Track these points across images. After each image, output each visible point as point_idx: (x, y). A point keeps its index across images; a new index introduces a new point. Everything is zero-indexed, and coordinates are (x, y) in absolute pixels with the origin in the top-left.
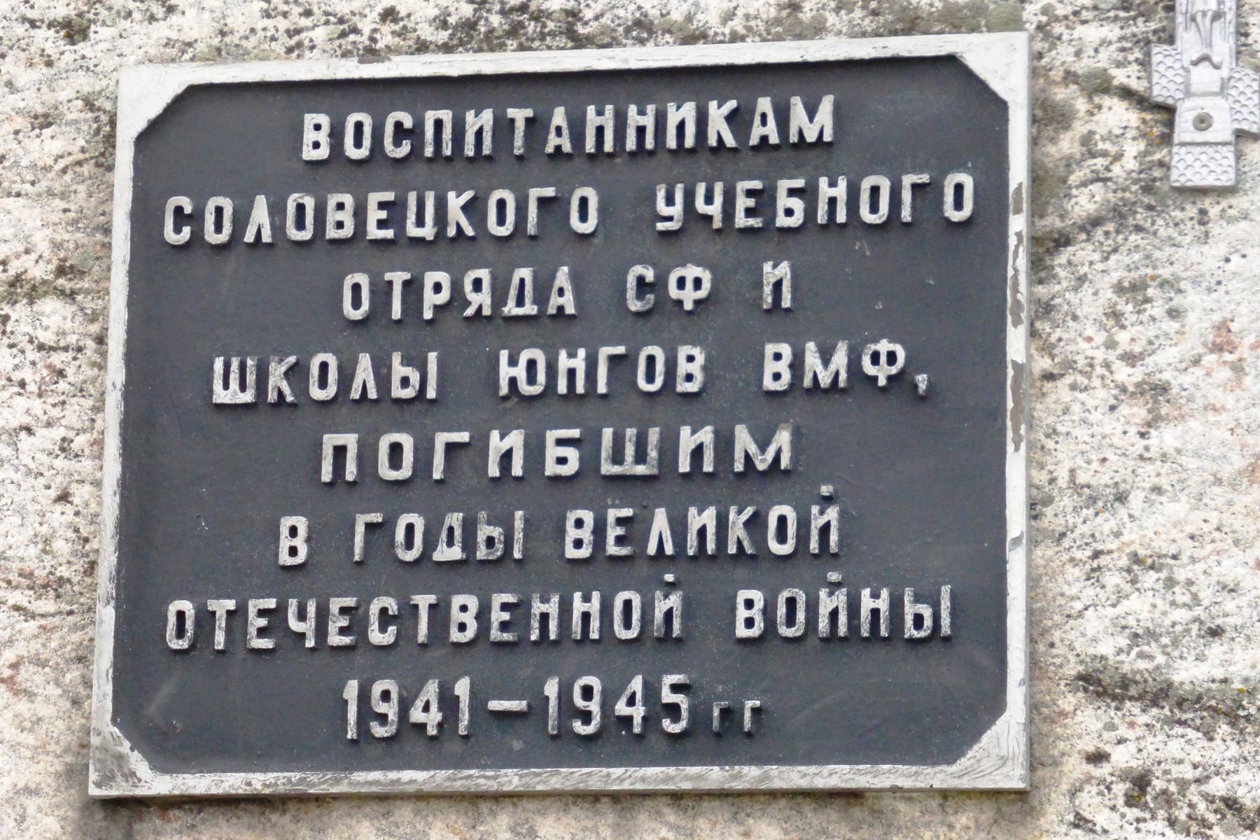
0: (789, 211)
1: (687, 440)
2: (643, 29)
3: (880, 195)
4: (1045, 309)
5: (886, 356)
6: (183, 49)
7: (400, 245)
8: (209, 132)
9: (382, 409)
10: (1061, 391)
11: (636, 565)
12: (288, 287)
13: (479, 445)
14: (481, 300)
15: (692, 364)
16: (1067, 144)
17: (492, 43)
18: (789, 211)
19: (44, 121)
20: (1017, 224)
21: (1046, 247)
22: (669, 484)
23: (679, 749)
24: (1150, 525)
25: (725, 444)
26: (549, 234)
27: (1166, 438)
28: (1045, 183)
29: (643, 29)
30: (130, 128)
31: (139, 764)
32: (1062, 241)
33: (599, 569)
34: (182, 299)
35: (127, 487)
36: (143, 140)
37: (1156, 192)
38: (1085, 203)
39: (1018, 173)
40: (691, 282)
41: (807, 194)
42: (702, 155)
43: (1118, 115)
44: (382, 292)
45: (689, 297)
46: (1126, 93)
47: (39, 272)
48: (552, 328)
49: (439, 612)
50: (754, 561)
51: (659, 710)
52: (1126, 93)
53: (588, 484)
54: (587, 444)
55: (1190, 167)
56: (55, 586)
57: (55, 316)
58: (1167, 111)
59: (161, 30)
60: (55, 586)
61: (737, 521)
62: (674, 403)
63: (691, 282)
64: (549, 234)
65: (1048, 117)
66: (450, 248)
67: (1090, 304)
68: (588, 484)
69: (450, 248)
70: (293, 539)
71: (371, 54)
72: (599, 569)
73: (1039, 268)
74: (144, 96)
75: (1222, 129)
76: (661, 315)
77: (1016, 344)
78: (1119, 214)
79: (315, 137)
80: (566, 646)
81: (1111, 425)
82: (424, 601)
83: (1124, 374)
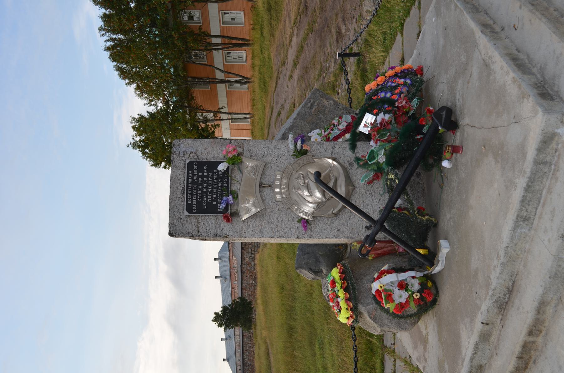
0: (196, 173)
3: (196, 168)
5: (205, 168)
7: (197, 197)
9: (207, 198)
11: (217, 182)
12: (199, 204)
15: (205, 179)
18: (196, 173)
22: (213, 180)
23: (228, 180)
26: (197, 188)
30: (188, 214)
33: (217, 184)
34: (200, 210)
35: (211, 213)
37: (196, 153)
38: (196, 157)
40: (200, 179)
42: (193, 179)
48: (202, 188)
53: (212, 185)
62: (208, 180)
63: (200, 179)
64: (197, 188)
67: (202, 157)
68: (212, 185)
70: (215, 203)
72: (217, 184)
74: (186, 213)
76: (202, 181)
79: (190, 202)
80: (222, 186)
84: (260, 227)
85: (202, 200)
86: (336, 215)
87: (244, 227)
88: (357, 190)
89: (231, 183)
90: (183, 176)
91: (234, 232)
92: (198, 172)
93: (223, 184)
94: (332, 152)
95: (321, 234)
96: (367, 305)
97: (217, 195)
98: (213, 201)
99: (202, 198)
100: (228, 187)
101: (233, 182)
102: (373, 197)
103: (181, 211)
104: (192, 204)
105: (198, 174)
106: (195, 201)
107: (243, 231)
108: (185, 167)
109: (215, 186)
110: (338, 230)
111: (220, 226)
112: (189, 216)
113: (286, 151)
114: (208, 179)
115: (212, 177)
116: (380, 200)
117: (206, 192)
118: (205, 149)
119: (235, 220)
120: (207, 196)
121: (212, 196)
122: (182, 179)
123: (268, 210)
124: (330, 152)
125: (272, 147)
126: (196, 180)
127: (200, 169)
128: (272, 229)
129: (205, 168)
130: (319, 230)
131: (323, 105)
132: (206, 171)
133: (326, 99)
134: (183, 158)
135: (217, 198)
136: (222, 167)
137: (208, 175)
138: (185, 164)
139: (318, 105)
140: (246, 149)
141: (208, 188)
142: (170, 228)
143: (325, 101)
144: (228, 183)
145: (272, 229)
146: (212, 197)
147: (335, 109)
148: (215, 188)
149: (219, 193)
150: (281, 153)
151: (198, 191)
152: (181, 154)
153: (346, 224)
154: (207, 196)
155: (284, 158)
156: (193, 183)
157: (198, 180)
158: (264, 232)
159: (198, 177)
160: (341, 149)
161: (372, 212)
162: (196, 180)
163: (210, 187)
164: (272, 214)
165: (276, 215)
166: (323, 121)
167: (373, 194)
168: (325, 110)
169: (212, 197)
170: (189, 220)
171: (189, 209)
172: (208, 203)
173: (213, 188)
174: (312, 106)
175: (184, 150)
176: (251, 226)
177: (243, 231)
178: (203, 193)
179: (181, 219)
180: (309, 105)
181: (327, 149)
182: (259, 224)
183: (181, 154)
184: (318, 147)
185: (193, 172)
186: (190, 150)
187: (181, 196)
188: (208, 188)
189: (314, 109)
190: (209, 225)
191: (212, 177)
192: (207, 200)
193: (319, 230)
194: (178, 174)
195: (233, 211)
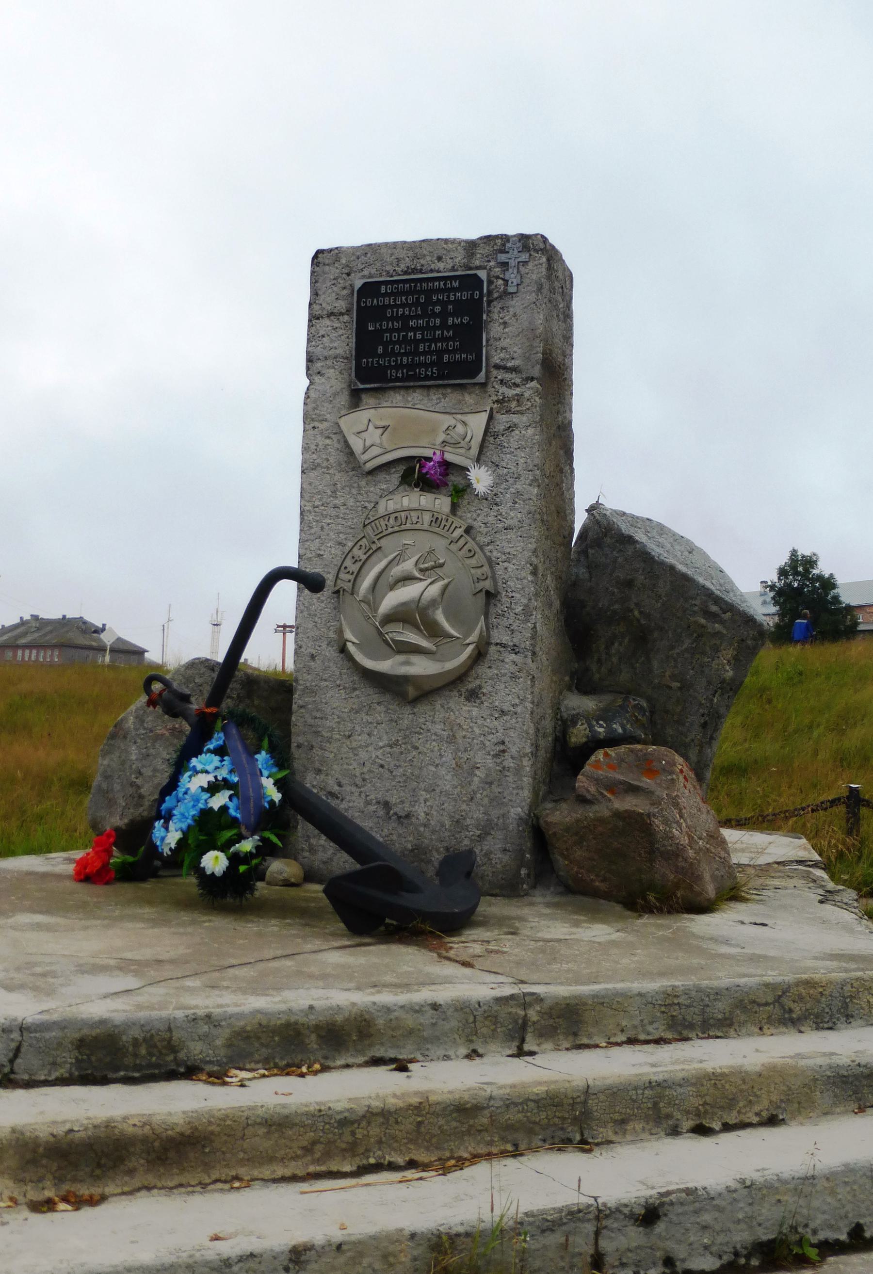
0: (452, 298)
1: (437, 333)
2: (432, 271)
3: (465, 295)
4: (490, 312)
5: (466, 320)
6: (364, 277)
7: (396, 306)
9: (393, 330)
10: (492, 324)
11: (430, 352)
13: (407, 334)
14: (407, 313)
15: (438, 321)
16: (493, 287)
17: (410, 274)
18: (452, 298)
19: (344, 288)
20: (485, 299)
21: (489, 302)
22: (435, 340)
24: (504, 343)
25: (443, 333)
26: (417, 303)
27: (507, 330)
28: (490, 292)
29: (432, 271)
30: (356, 289)
31: (359, 384)
32: (492, 301)
33: (424, 353)
35: (356, 342)
36: (358, 291)
37: (506, 293)
38: (496, 295)
39: (485, 291)
40: (438, 309)
41: (455, 295)
42: (440, 291)
43: (500, 282)
44: (393, 312)
45: (438, 311)
46: (502, 279)
47: (344, 311)
48: (417, 317)
49: (401, 360)
50: (447, 351)
51: (432, 373)
52: (502, 279)
53: (423, 340)
54: (423, 334)
55: (512, 289)
56: (347, 358)
57: (346, 318)
58: (507, 281)
59: (361, 274)
60: (347, 358)
61: (444, 345)
62: (435, 328)
63: (438, 309)
64: (417, 303)
65: (490, 282)
66: (403, 306)
67: (496, 310)
68: (423, 340)
69: (403, 306)
70: (380, 350)
71: (392, 276)
72: (424, 353)
73: (489, 305)
74: (358, 284)
75: (515, 284)
76: (434, 315)
77: (485, 317)
78: (500, 297)
79: (383, 290)
80: (420, 365)
81: (499, 329)
83: (501, 321)
84: (325, 464)
85: (388, 319)
86: (343, 650)
88: (408, 709)
89: (428, 387)
90: (449, 266)
91: (315, 401)
92: (456, 302)
93: (425, 365)
94: (504, 646)
95: (305, 613)
96: (136, 717)
97: (399, 354)
98: (385, 345)
99: (393, 318)
102: (388, 749)
103: (366, 272)
104: (378, 295)
105: (449, 302)
106: (387, 302)
107: (316, 424)
108: (470, 269)
109: (421, 348)
110: (313, 657)
112: (353, 291)
113: (508, 523)
114: (438, 328)
115: (443, 339)
116: (382, 766)
117: (406, 328)
120: (398, 330)
122: (441, 265)
123: (363, 483)
124: (505, 639)
125: (518, 486)
126: (435, 298)
127: (461, 308)
128: (319, 493)
129: (466, 320)
130: (313, 608)
131: (716, 649)
132: (457, 321)
133: (736, 658)
134: (492, 263)
135: (393, 354)
137: (449, 328)
138: (478, 268)
139: (717, 634)
140: (515, 418)
141: (414, 329)
142: (330, 251)
143: (728, 653)
145: (319, 493)
146: (395, 343)
147: (709, 683)
148: (417, 347)
149: (405, 359)
150: (503, 510)
151: (410, 306)
152: (502, 257)
153: (326, 676)
154: (398, 330)
155: (491, 519)
156: (429, 293)
157: (436, 304)
158: (313, 474)
159: (444, 304)
160: (513, 668)
161: (354, 744)
162: (435, 298)
164: (354, 491)
165: (351, 502)
166: (672, 648)
167: (396, 750)
168: (703, 653)
169: (395, 343)
170: (345, 292)
171: (369, 289)
172: (379, 332)
173: (417, 342)
174: (707, 614)
175: (512, 263)
176: (328, 441)
177: (316, 424)
178: (405, 319)
179: (348, 274)
180: (714, 608)
181: (513, 631)
182: (332, 460)
183: (502, 257)
184: (519, 609)
185: (453, 289)
186: (512, 276)
187: (403, 266)
188: (414, 329)
189: (703, 621)
190: (332, 341)
191: (443, 339)
192: (387, 330)
193: (313, 608)
194: (453, 255)
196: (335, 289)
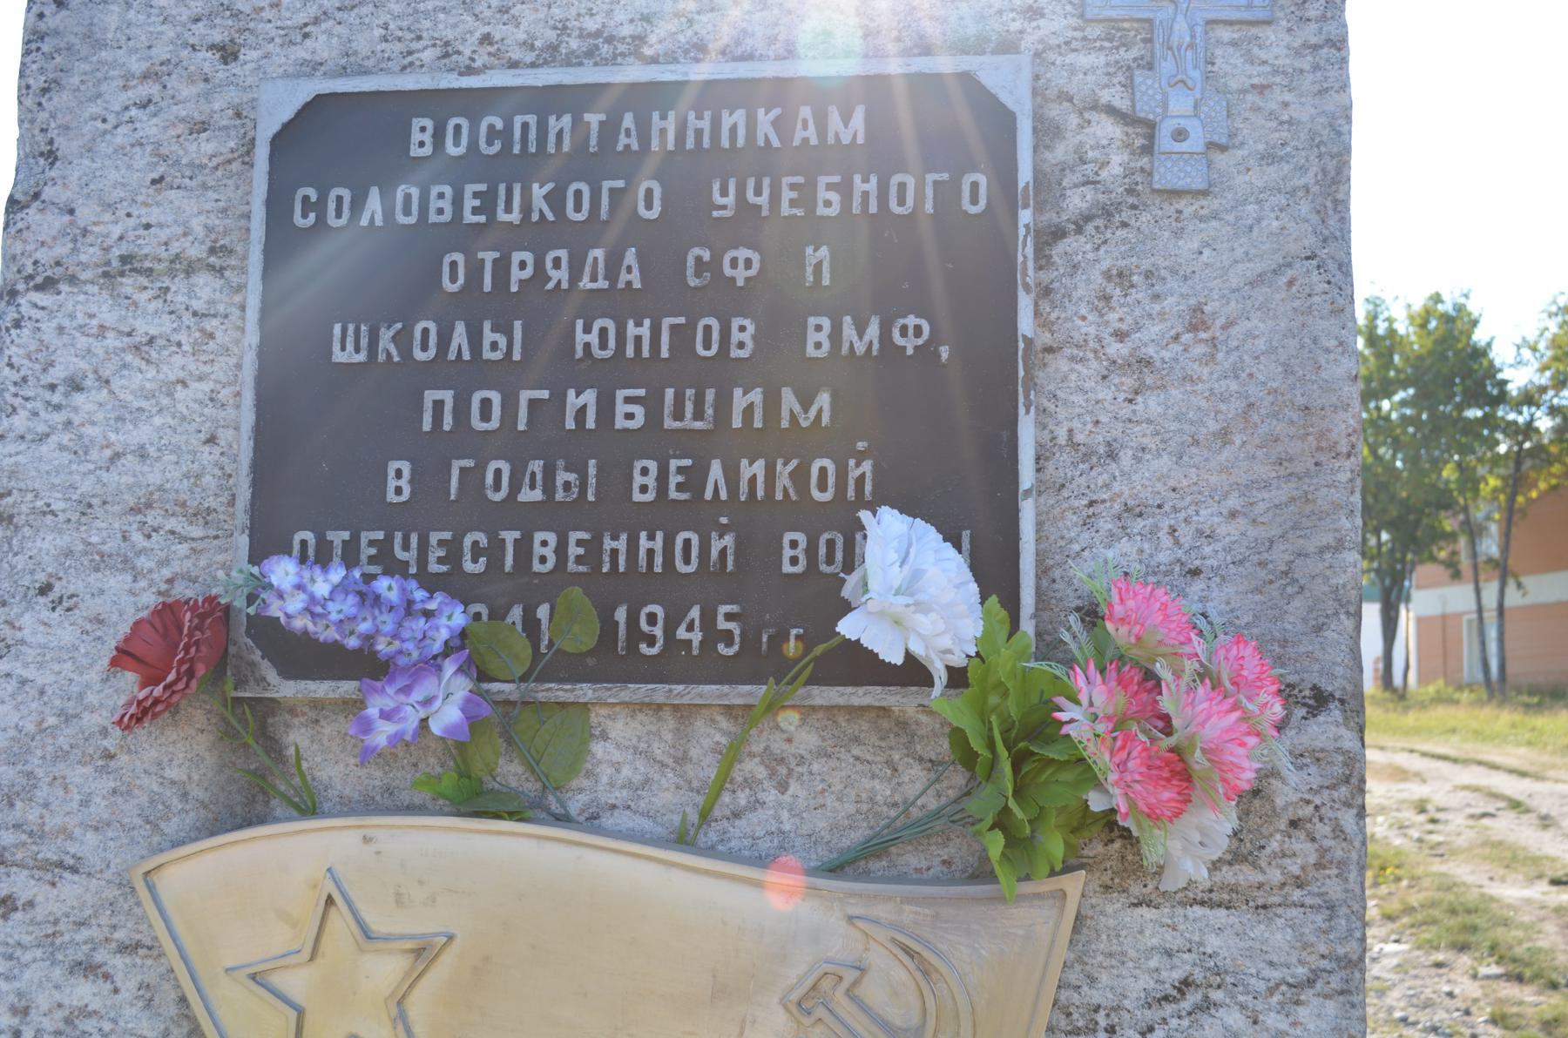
0: (829, 203)
1: (739, 400)
4: (1046, 291)
6: (312, 67)
8: (333, 140)
10: (1061, 364)
13: (559, 399)
14: (561, 276)
15: (744, 332)
16: (1061, 152)
17: (571, 61)
19: (200, 127)
20: (1025, 216)
21: (1050, 236)
24: (1138, 479)
25: (772, 404)
27: (1151, 404)
30: (268, 128)
31: (272, 675)
32: (1058, 234)
33: (663, 515)
35: (259, 431)
36: (276, 140)
38: (1077, 201)
39: (1025, 175)
41: (845, 189)
43: (1106, 129)
44: (475, 271)
45: (741, 275)
46: (1111, 110)
47: (196, 252)
48: (618, 303)
49: (524, 547)
51: (713, 636)
52: (1111, 110)
54: (652, 405)
55: (1168, 175)
56: (202, 515)
57: (205, 287)
58: (1150, 128)
59: (300, 53)
60: (202, 515)
61: (784, 471)
65: (1046, 132)
68: (654, 440)
70: (399, 481)
71: (469, 71)
72: (663, 515)
73: (1043, 259)
74: (280, 104)
75: (1195, 143)
77: (1026, 324)
81: (1104, 394)
82: (510, 536)
83: (1115, 349)
87: (71, 890)
97: (511, 511)
98: (430, 458)
99: (476, 306)
100: (614, 660)
101: (709, 736)
103: (322, 46)
109: (643, 483)
111: (101, 561)
118: (1197, 321)
119: (181, 755)
120: (506, 375)
121: (516, 447)
136: (912, 589)
140: (1220, 934)
141: (607, 376)
144: (676, 665)
146: (481, 447)
148: (617, 478)
149: (544, 542)
154: (506, 375)
163: (629, 415)
170: (205, 147)
173: (618, 452)
176: (83, 992)
179: (228, 53)
188: (607, 376)
190: (124, 415)
192: (441, 370)
195: (297, 738)
196: (150, 127)
